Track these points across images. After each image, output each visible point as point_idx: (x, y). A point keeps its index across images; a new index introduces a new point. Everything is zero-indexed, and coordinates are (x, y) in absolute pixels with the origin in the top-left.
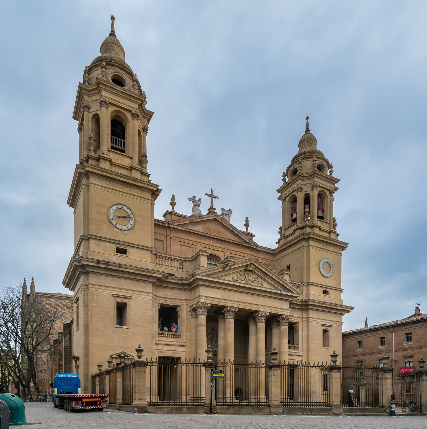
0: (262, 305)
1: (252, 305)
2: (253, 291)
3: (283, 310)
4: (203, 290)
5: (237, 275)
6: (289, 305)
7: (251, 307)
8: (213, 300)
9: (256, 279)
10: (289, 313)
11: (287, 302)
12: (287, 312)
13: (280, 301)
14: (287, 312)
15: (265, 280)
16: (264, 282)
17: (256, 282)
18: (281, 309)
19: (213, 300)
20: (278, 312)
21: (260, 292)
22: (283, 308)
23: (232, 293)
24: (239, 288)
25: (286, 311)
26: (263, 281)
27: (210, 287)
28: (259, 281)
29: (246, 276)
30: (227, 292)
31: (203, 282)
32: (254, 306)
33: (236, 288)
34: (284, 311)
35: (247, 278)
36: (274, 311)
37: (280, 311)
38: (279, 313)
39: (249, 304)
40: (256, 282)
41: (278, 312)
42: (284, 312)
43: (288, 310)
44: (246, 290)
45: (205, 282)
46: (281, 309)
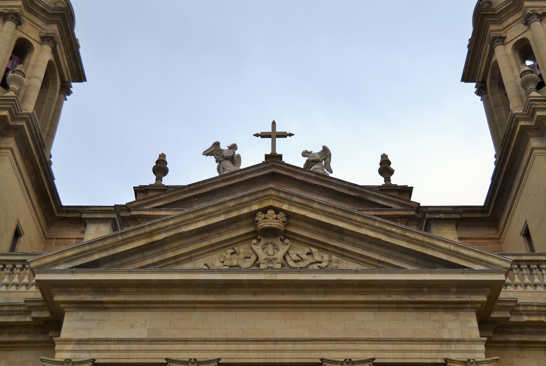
0: (337, 340)
1: (290, 346)
2: (283, 293)
3: (445, 347)
4: (78, 321)
5: (222, 256)
6: (474, 323)
7: (287, 355)
8: (109, 351)
9: (304, 256)
10: (479, 352)
11: (463, 315)
12: (474, 352)
13: (427, 314)
14: (474, 352)
15: (343, 254)
16: (345, 262)
17: (302, 264)
18: (433, 341)
19: (109, 351)
20: (424, 355)
21: (317, 293)
22: (446, 336)
23: (197, 316)
24: (220, 293)
25: (463, 347)
26: (334, 258)
27: (105, 309)
28: (317, 258)
29: (259, 251)
30: (177, 315)
31: (70, 293)
32: (299, 346)
33: (207, 293)
34: (453, 347)
35: (262, 256)
36: (400, 355)
37: (431, 351)
38: (429, 361)
39: (276, 341)
40: (302, 264)
41: (424, 355)
42: (456, 351)
43: (473, 341)
44: (255, 294)
45: (79, 293)
46: (433, 341)
